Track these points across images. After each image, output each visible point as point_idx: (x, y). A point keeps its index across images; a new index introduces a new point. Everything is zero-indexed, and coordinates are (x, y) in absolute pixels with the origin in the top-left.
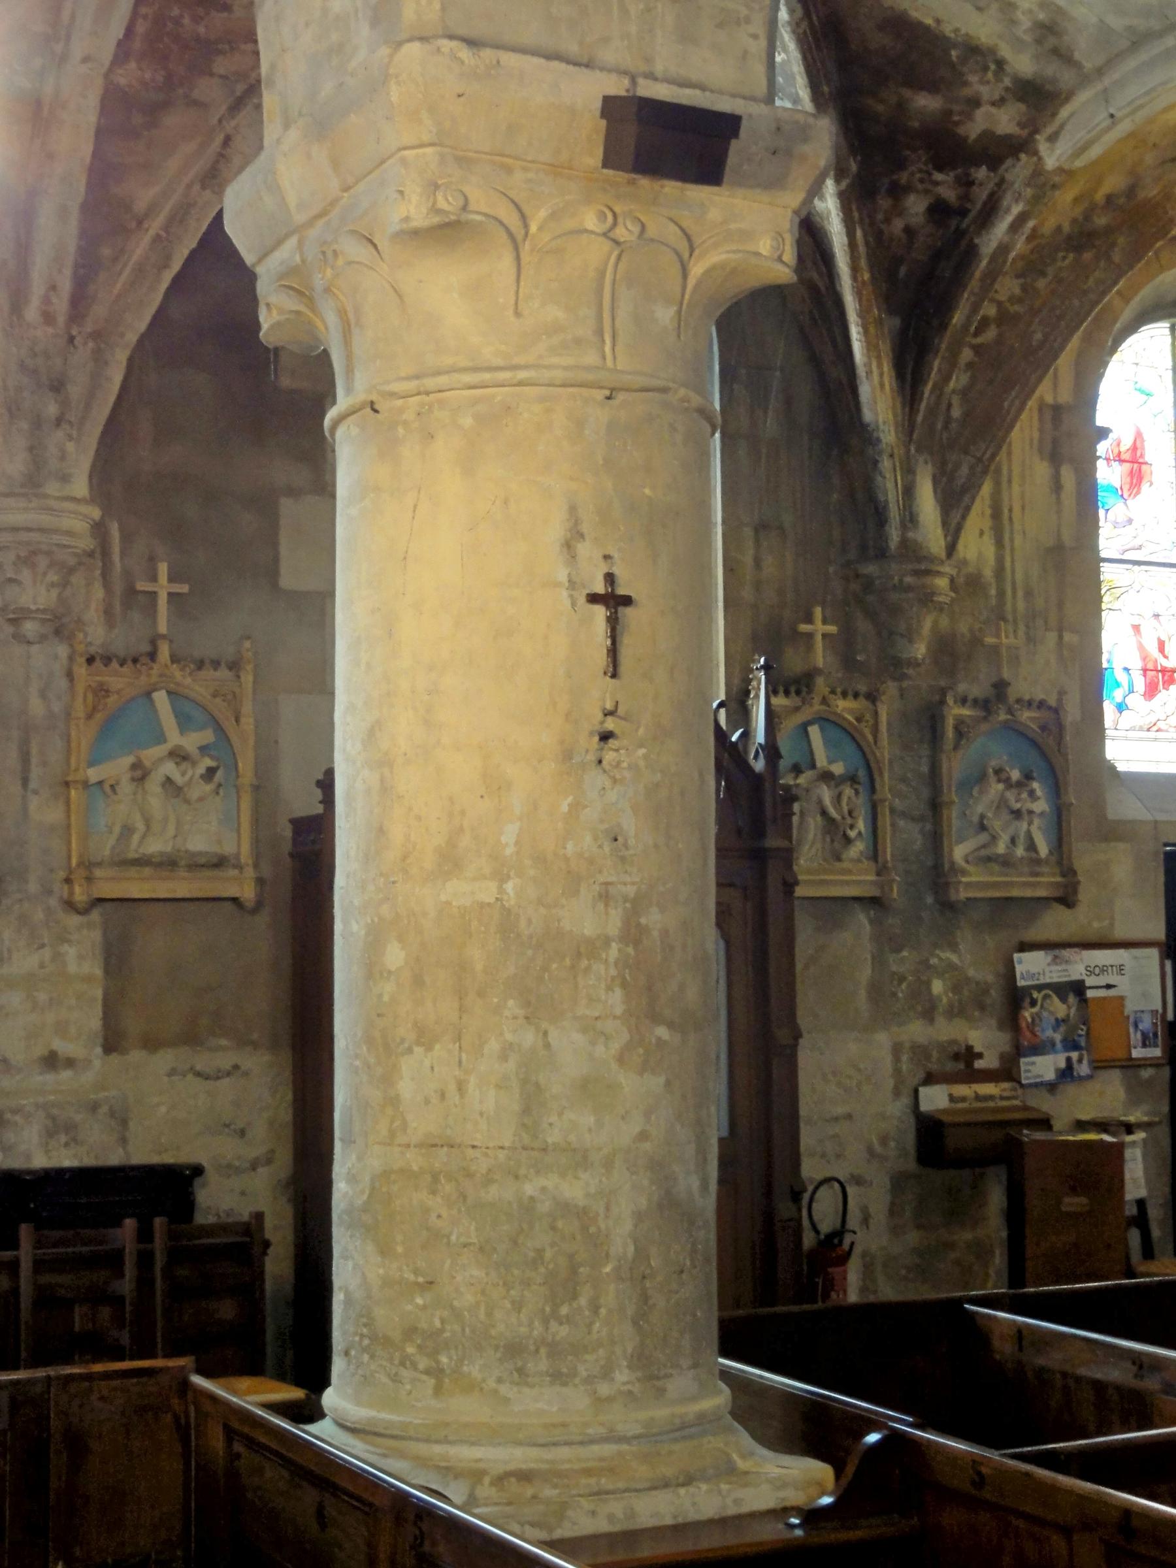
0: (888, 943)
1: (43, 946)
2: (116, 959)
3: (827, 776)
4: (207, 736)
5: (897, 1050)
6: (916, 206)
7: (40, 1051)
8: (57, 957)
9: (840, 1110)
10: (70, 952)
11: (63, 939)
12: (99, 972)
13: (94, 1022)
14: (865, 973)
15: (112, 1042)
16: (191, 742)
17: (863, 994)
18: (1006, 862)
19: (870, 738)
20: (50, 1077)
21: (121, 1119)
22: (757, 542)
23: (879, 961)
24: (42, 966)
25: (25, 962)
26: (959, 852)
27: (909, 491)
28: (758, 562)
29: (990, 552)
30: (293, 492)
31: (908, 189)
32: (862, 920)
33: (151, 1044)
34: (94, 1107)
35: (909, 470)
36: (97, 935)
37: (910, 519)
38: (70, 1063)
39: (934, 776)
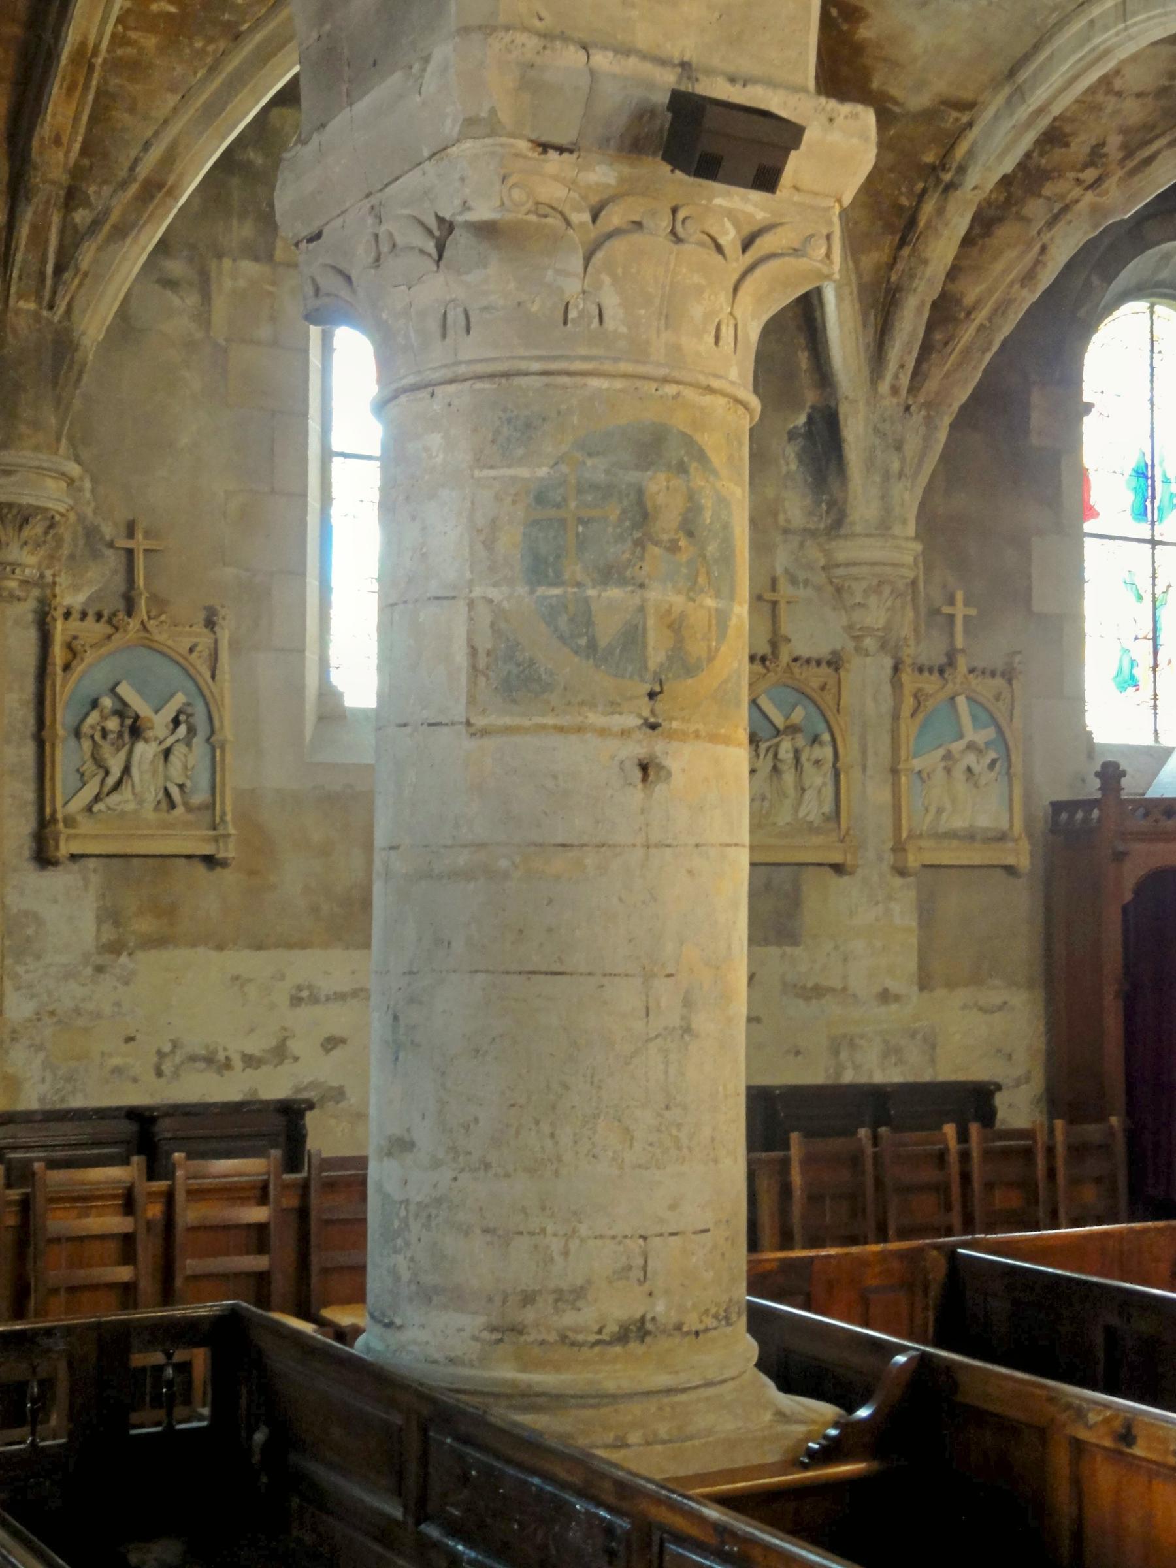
1: (877, 903)
7: (877, 989)
10: (896, 907)
11: (890, 898)
12: (914, 924)
13: (912, 965)
15: (924, 983)
16: (981, 736)
21: (931, 1044)
24: (877, 919)
33: (951, 985)
36: (912, 894)
38: (897, 998)
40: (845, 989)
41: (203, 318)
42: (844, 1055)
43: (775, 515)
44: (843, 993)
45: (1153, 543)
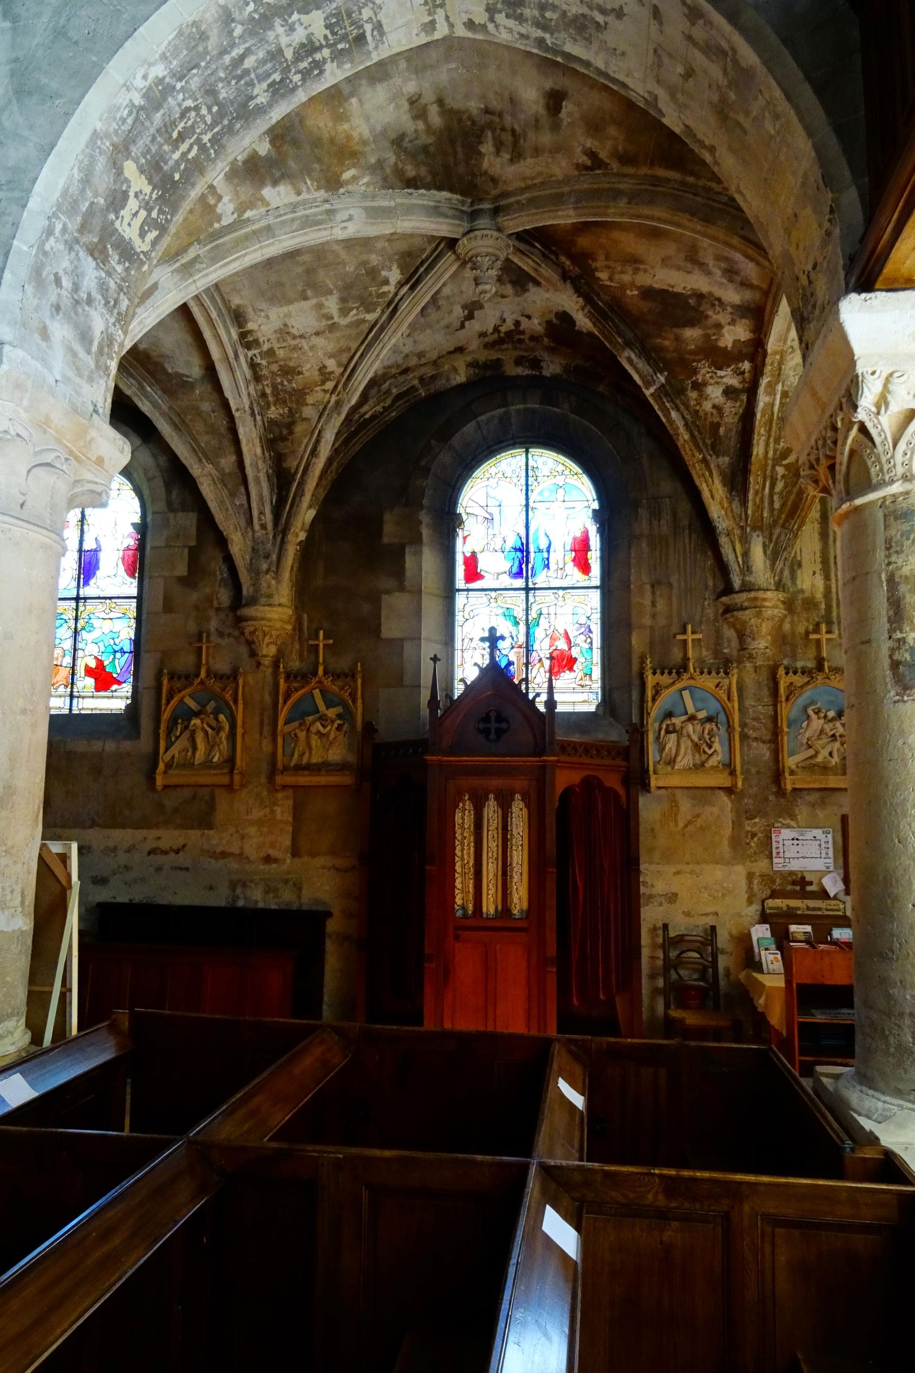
0: (743, 815)
1: (266, 806)
2: (298, 812)
3: (692, 718)
4: (339, 709)
5: (750, 876)
6: (715, 393)
8: (273, 812)
9: (710, 909)
11: (275, 804)
12: (290, 819)
13: (287, 841)
14: (727, 831)
15: (295, 852)
16: (332, 713)
17: (726, 842)
18: (825, 769)
19: (726, 699)
20: (267, 867)
21: (298, 887)
22: (653, 593)
23: (737, 824)
24: (265, 816)
25: (257, 814)
26: (791, 762)
27: (746, 554)
28: (654, 604)
29: (820, 583)
30: (388, 592)
31: (705, 384)
32: (725, 800)
33: (313, 854)
34: (286, 882)
35: (745, 540)
36: (290, 803)
37: (747, 568)
38: (276, 860)
39: (775, 718)
40: (241, 854)
42: (239, 891)
43: (212, 601)
44: (241, 856)
45: (527, 589)
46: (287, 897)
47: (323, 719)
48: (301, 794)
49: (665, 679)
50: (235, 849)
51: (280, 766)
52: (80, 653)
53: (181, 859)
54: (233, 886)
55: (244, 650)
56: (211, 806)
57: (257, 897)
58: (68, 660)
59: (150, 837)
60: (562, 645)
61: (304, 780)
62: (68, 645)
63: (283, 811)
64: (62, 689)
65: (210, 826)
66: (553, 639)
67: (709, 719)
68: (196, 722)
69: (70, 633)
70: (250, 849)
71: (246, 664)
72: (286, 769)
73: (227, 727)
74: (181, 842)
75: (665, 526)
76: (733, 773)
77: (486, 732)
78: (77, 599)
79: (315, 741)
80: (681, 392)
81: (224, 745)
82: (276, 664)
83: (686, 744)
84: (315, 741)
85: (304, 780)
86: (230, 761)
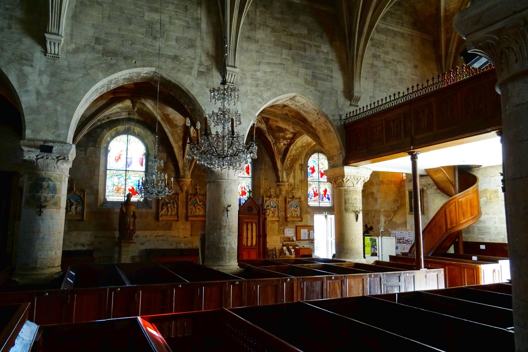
0: (280, 226)
5: (281, 238)
6: (282, 144)
13: (190, 233)
14: (277, 229)
15: (191, 235)
16: (200, 204)
18: (294, 217)
21: (192, 243)
23: (279, 228)
25: (182, 227)
26: (288, 216)
27: (283, 175)
29: (293, 180)
32: (276, 223)
35: (283, 172)
37: (283, 178)
39: (286, 207)
41: (86, 154)
46: (190, 246)
47: (199, 205)
48: (193, 223)
49: (267, 199)
50: (177, 235)
51: (189, 215)
52: (127, 185)
53: (164, 238)
54: (177, 244)
55: (178, 188)
56: (171, 225)
57: (183, 246)
58: (123, 187)
59: (156, 233)
60: (243, 190)
61: (194, 219)
62: (123, 183)
63: (188, 226)
64: (122, 195)
65: (171, 230)
66: (242, 188)
67: (275, 207)
68: (169, 205)
69: (124, 179)
70: (181, 235)
71: (179, 191)
72: (190, 216)
73: (176, 206)
74: (163, 234)
75: (267, 167)
76: (279, 218)
77: (248, 210)
78: (126, 171)
79: (197, 210)
80: (277, 143)
81: (176, 211)
82: (187, 192)
83: (271, 212)
84: (197, 210)
85: (194, 219)
86: (177, 214)
